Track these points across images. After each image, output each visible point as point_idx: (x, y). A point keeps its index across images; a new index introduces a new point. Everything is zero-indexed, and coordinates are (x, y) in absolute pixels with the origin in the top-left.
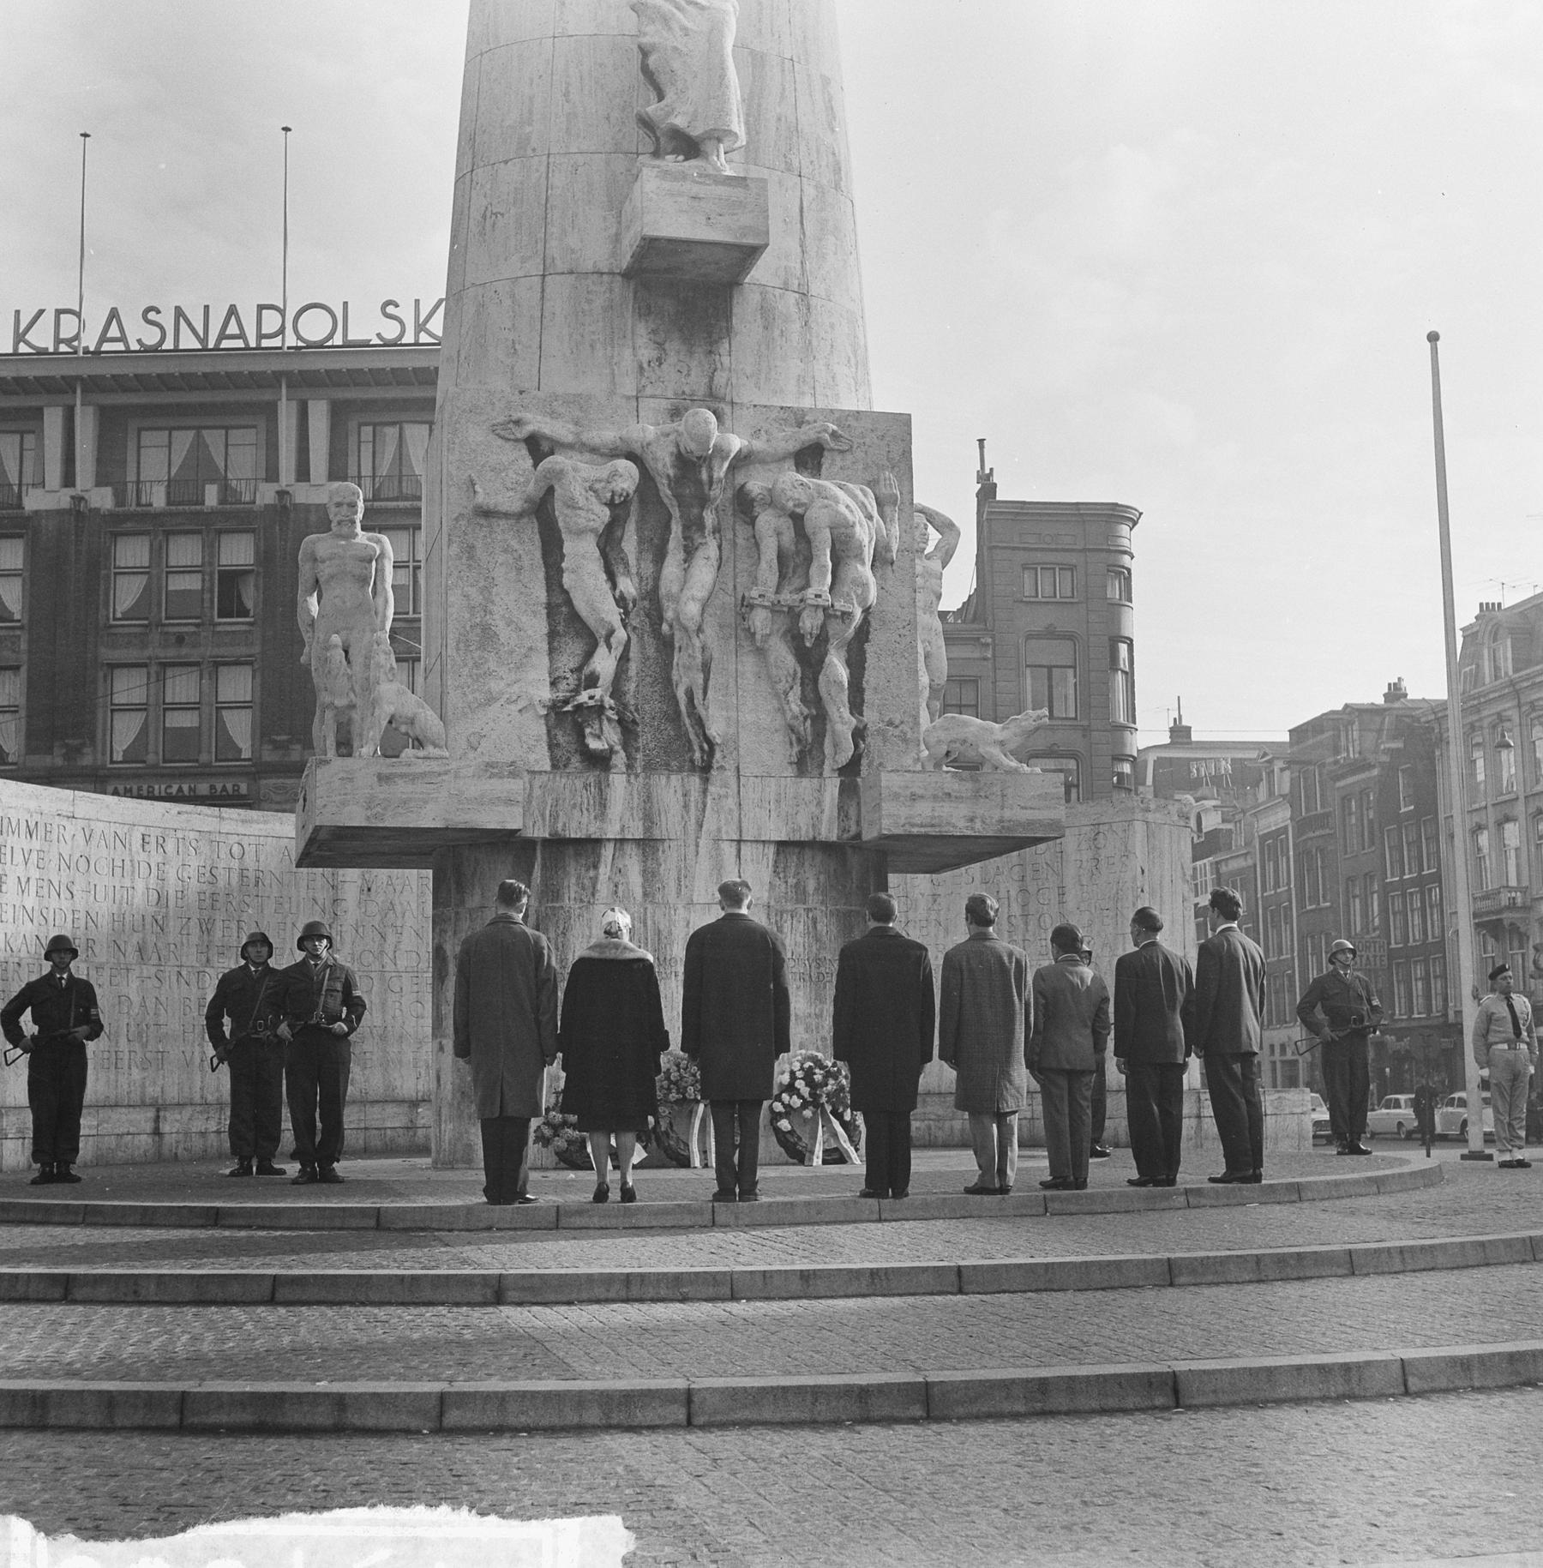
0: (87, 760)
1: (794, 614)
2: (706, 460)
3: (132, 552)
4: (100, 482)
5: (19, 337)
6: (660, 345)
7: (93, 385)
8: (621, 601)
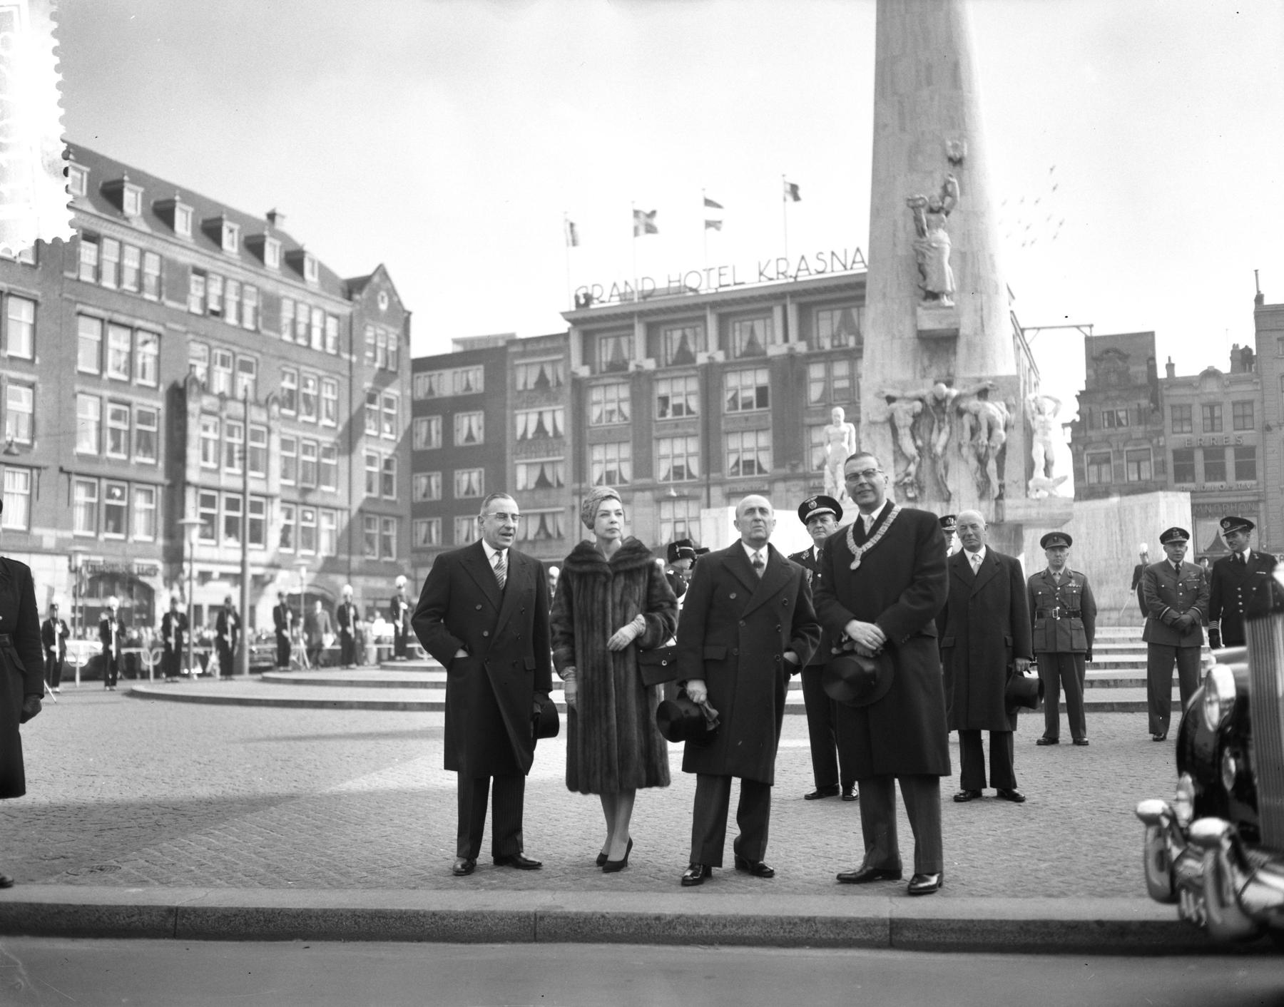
0: (801, 470)
2: (944, 400)
3: (816, 371)
4: (801, 338)
5: (761, 274)
6: (930, 360)
8: (917, 448)
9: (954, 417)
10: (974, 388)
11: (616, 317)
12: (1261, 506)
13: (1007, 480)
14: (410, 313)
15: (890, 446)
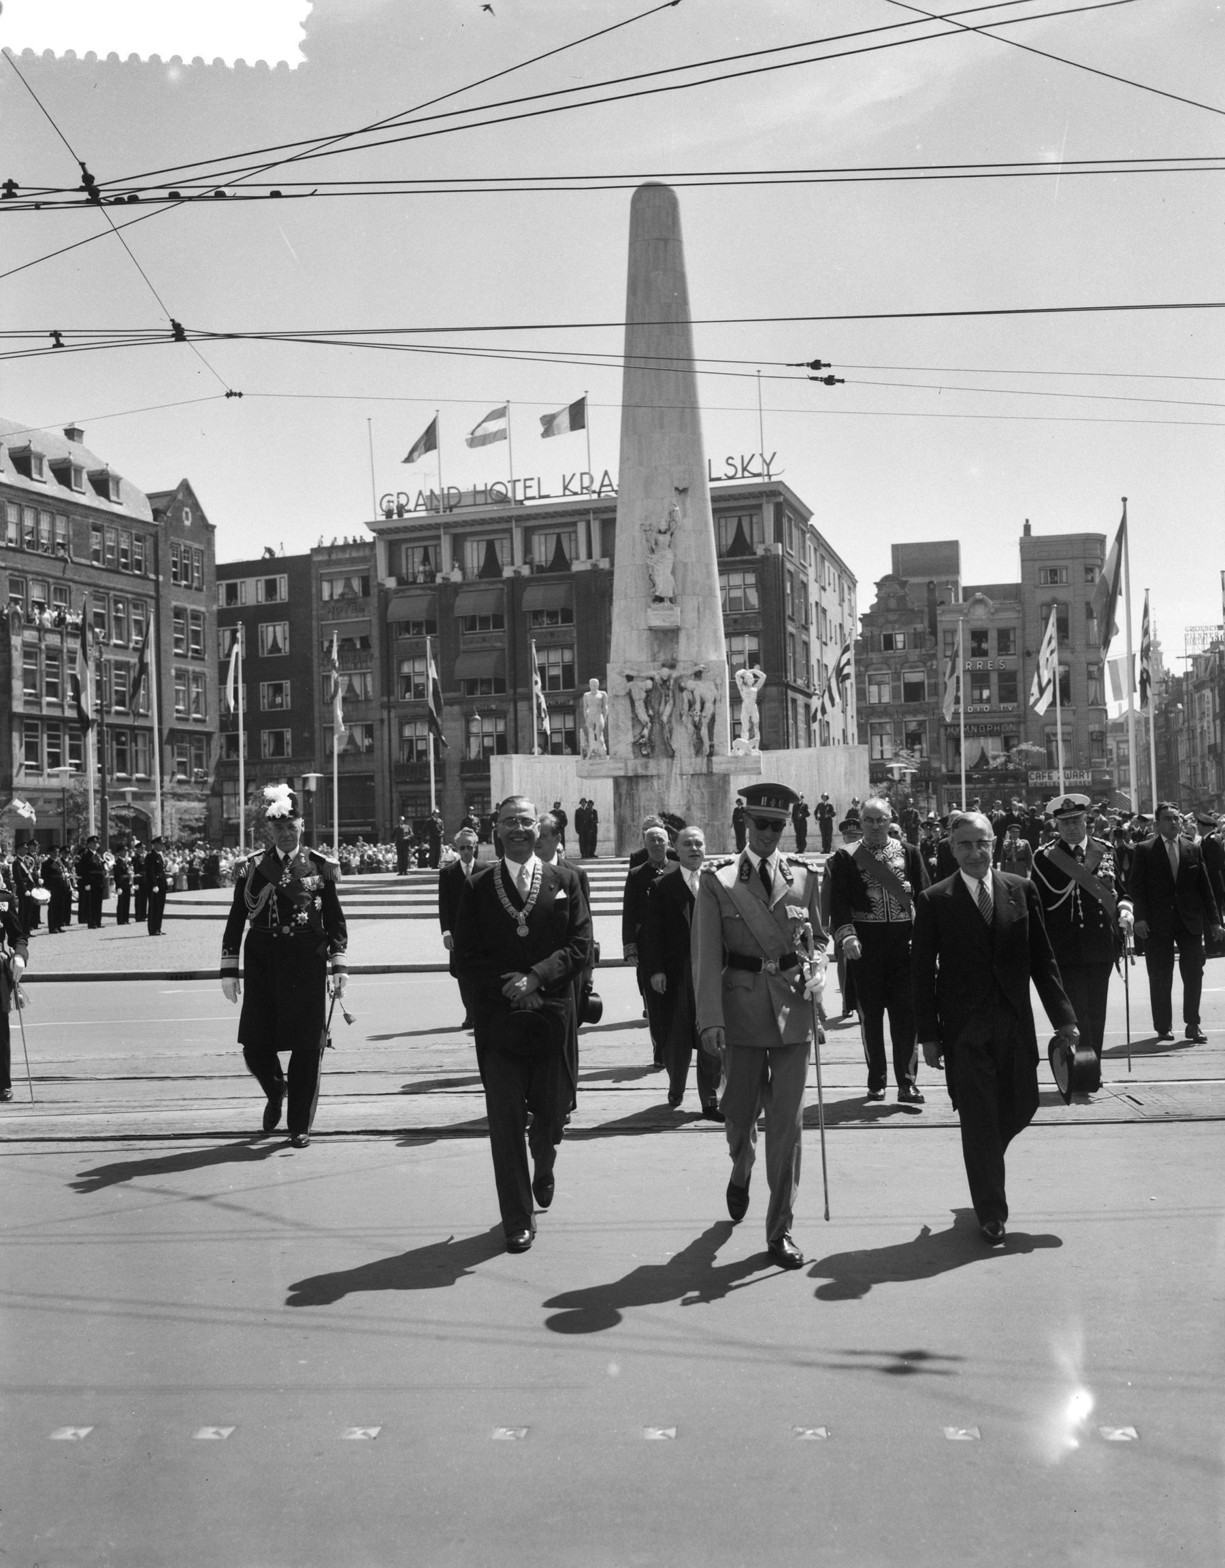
1: (692, 716)
4: (604, 555)
5: (565, 488)
6: (660, 646)
7: (597, 511)
9: (677, 692)
10: (691, 671)
11: (422, 528)
12: (1022, 727)
13: (716, 742)
14: (214, 527)
15: (630, 715)
